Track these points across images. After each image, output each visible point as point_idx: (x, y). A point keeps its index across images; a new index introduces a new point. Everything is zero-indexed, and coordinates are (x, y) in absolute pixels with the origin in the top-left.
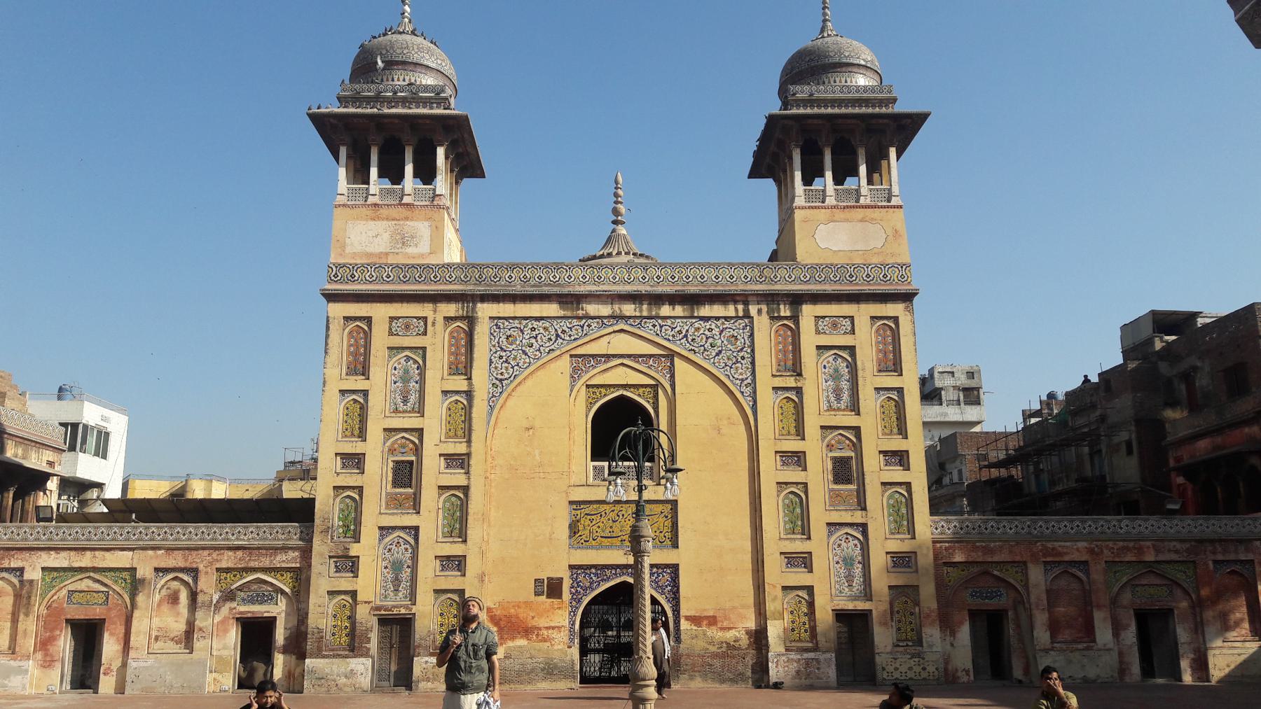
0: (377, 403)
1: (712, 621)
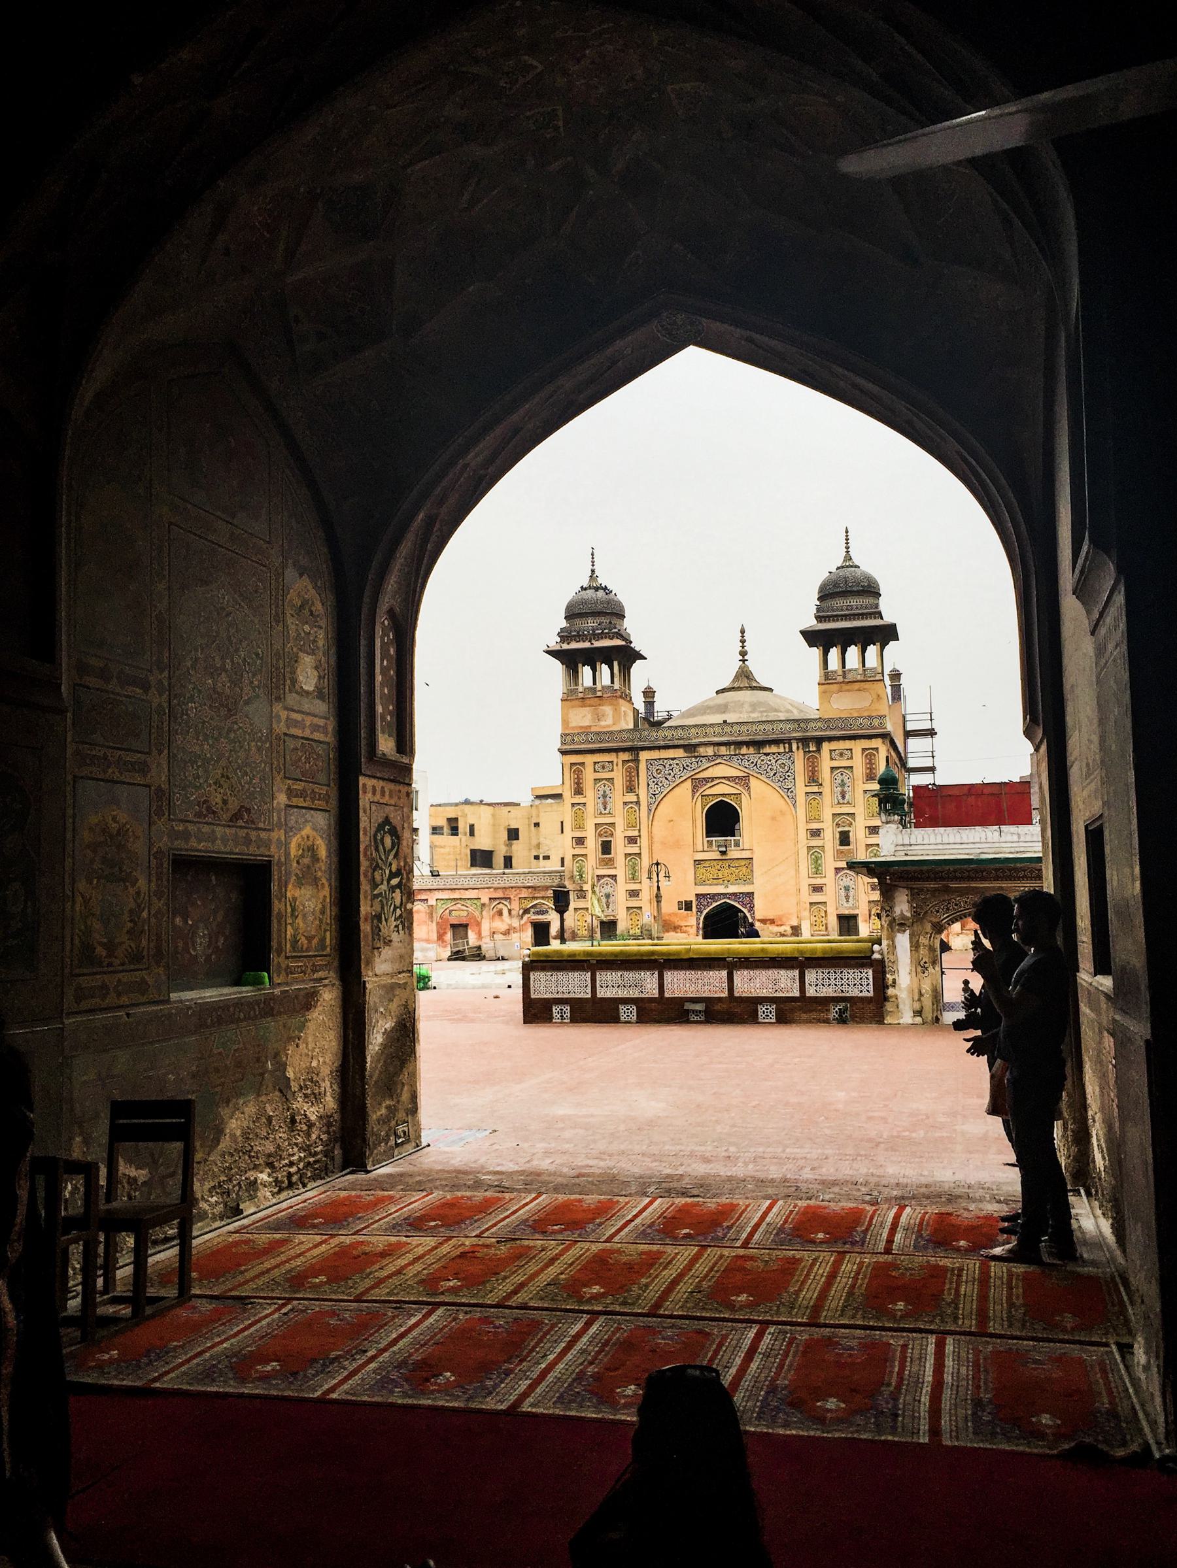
0: (590, 808)
1: (772, 922)
